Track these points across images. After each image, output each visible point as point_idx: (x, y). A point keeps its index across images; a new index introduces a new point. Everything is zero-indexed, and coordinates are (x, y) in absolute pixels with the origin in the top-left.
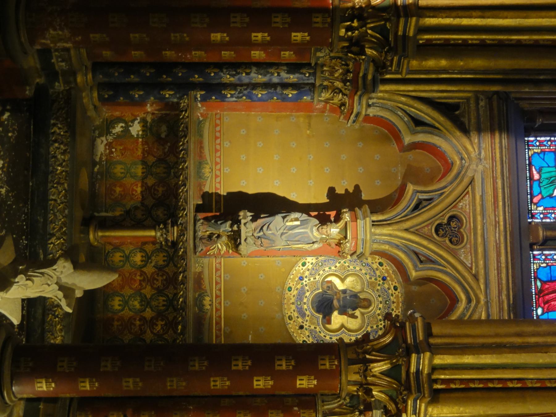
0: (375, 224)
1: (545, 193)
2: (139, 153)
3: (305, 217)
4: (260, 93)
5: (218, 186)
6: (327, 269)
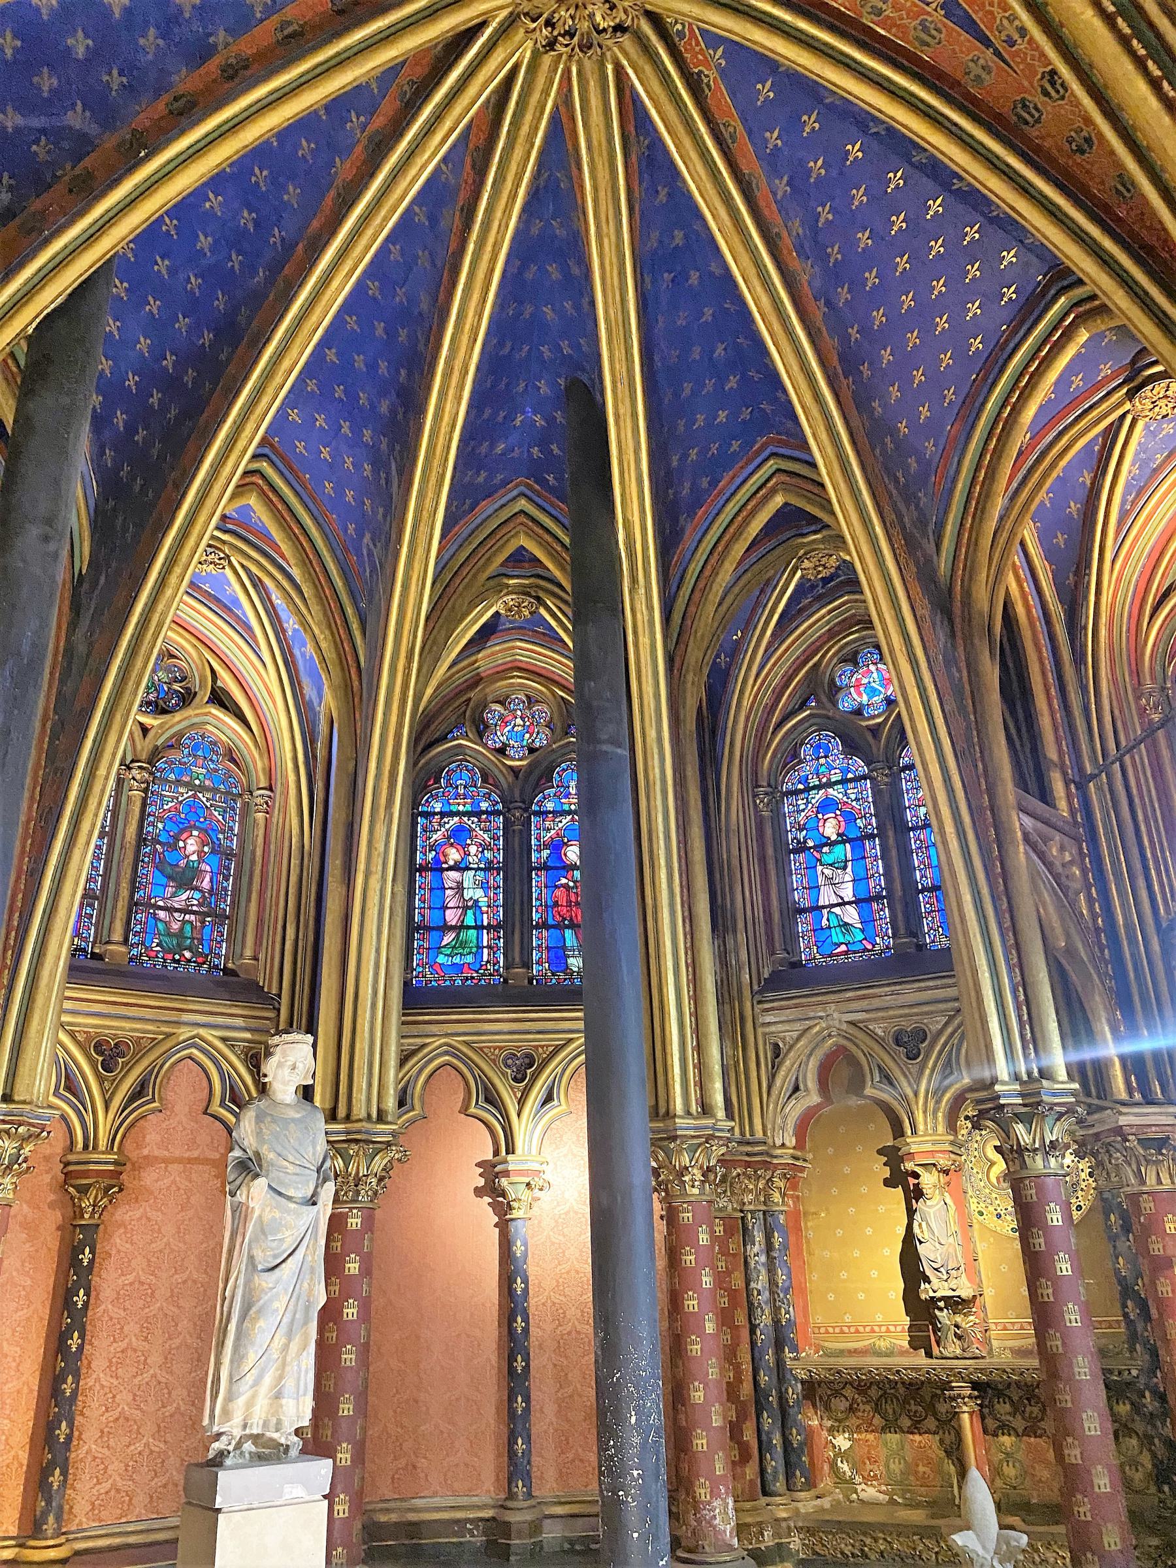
0: (914, 1132)
1: (860, 936)
2: (871, 1437)
3: (917, 1216)
4: (781, 1278)
5: (899, 1329)
6: (982, 1184)
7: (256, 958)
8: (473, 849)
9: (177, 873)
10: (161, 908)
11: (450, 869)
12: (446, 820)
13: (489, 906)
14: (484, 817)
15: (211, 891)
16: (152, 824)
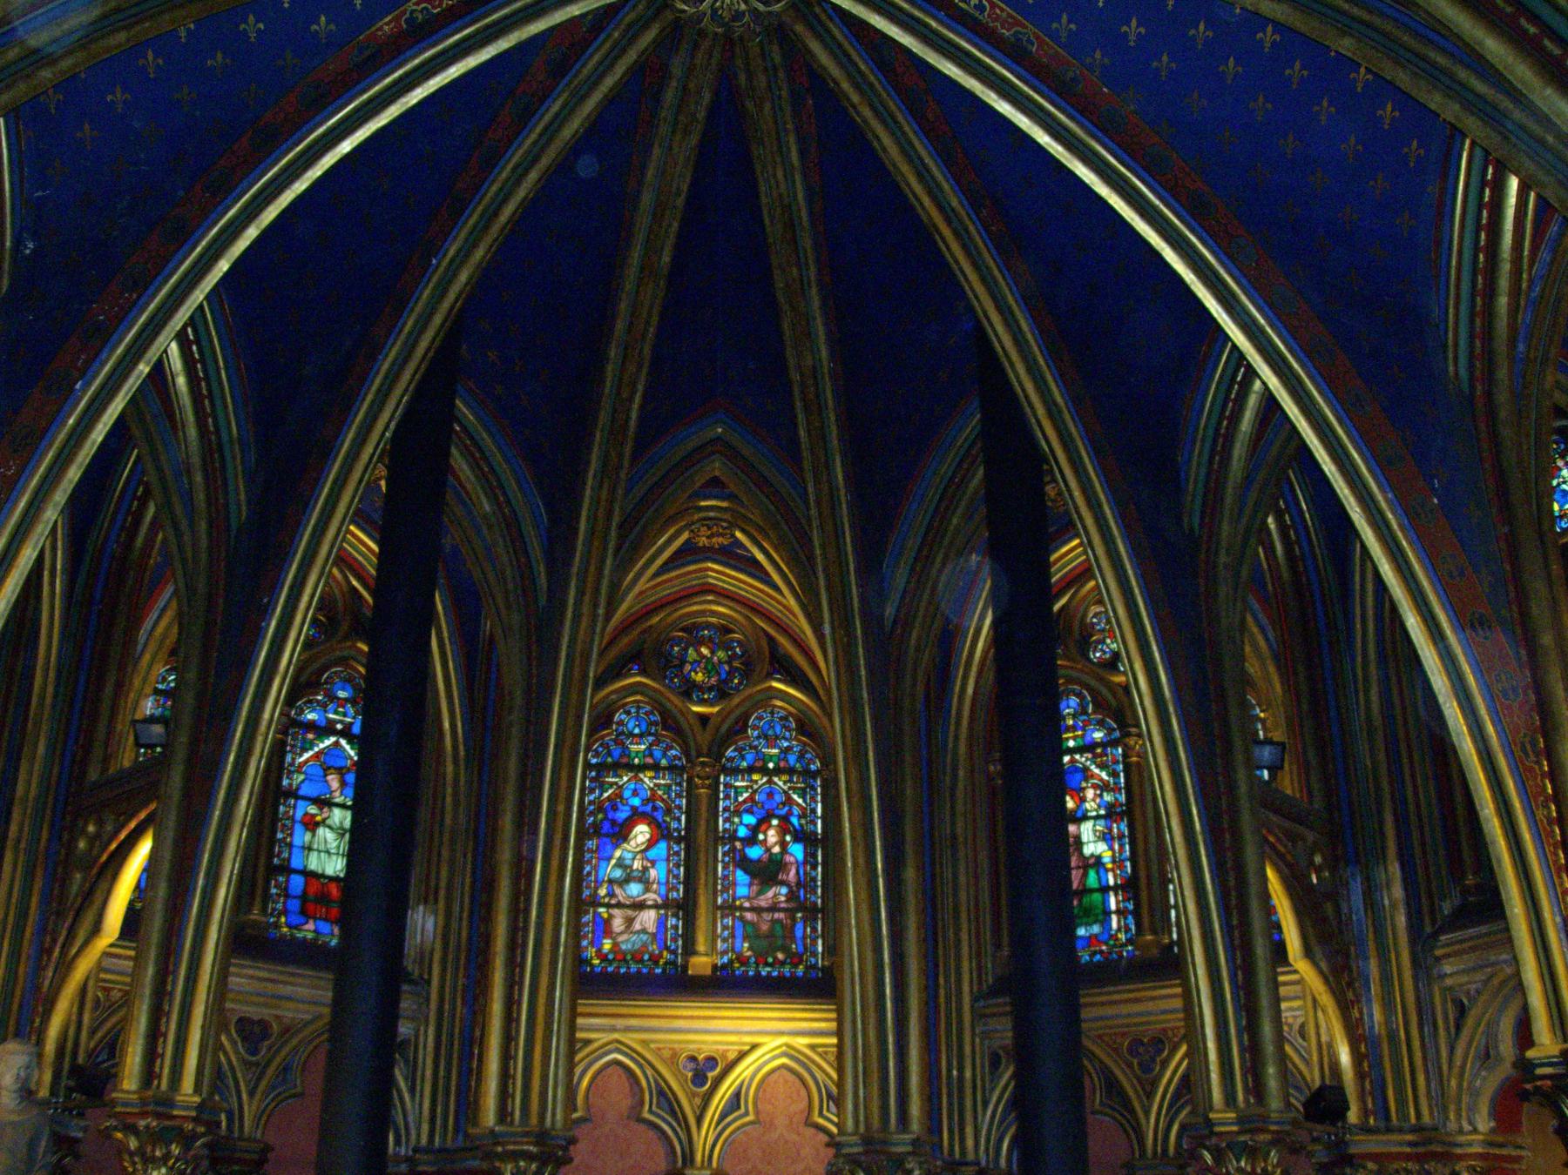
8: (1090, 793)
13: (1114, 862)
15: (799, 884)
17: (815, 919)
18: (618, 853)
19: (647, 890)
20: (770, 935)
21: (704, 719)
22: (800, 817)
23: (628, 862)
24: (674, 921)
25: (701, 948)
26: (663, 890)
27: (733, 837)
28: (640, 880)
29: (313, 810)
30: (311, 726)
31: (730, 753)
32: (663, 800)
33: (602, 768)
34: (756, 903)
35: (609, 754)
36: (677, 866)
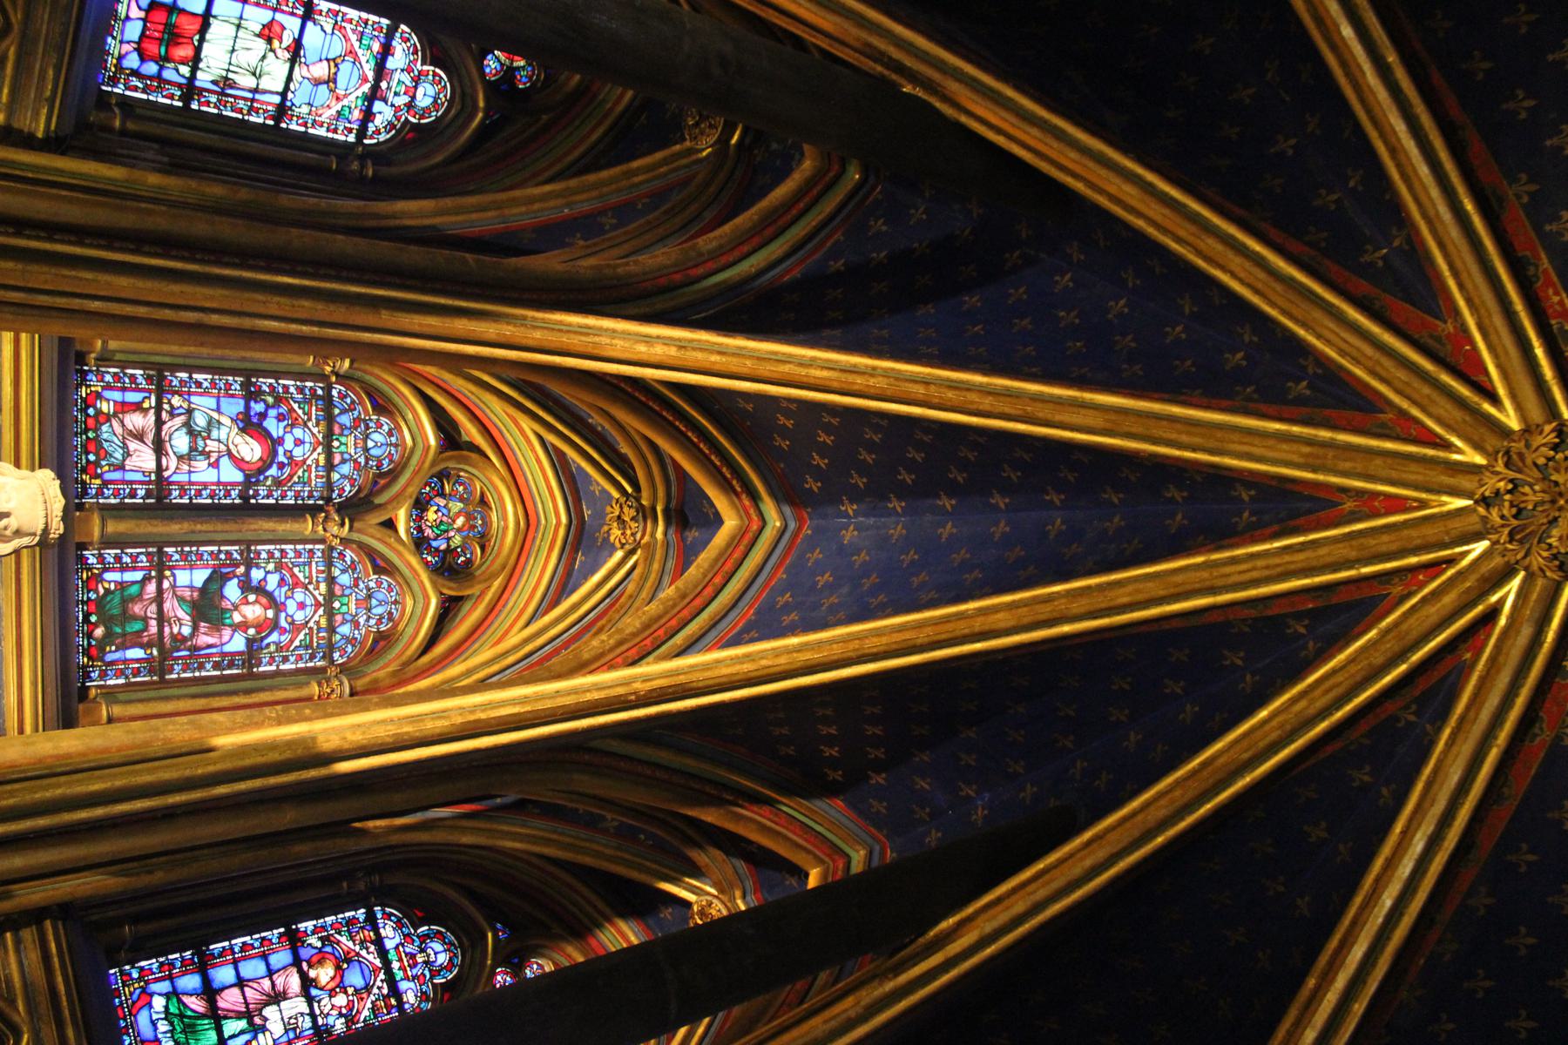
7: (110, 720)
8: (341, 1000)
9: (211, 599)
10: (160, 584)
11: (304, 977)
12: (372, 948)
14: (393, 1002)
15: (196, 648)
16: (271, 554)
17: (151, 672)
18: (225, 420)
19: (180, 458)
20: (126, 617)
21: (390, 525)
22: (277, 644)
23: (215, 434)
24: (141, 493)
25: (112, 527)
26: (185, 478)
27: (249, 565)
28: (193, 449)
29: (288, 39)
30: (386, 50)
31: (349, 554)
32: (291, 476)
33: (328, 399)
34: (168, 595)
35: (343, 412)
36: (212, 496)
